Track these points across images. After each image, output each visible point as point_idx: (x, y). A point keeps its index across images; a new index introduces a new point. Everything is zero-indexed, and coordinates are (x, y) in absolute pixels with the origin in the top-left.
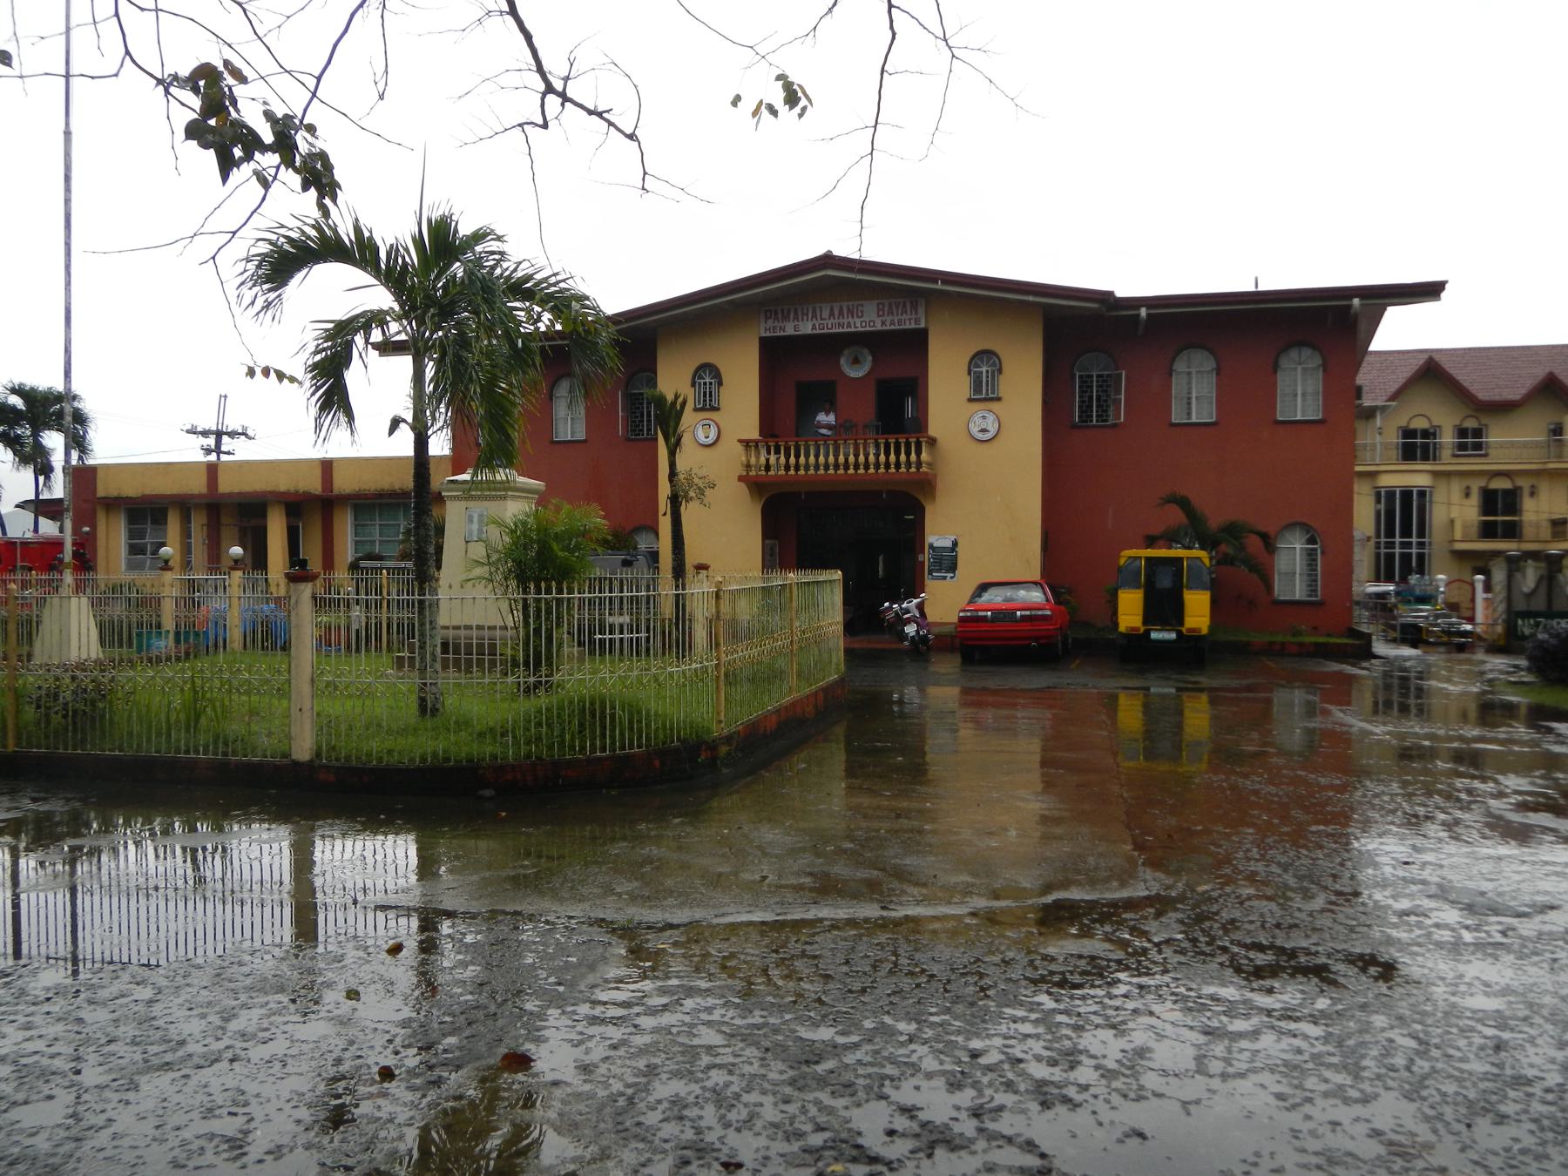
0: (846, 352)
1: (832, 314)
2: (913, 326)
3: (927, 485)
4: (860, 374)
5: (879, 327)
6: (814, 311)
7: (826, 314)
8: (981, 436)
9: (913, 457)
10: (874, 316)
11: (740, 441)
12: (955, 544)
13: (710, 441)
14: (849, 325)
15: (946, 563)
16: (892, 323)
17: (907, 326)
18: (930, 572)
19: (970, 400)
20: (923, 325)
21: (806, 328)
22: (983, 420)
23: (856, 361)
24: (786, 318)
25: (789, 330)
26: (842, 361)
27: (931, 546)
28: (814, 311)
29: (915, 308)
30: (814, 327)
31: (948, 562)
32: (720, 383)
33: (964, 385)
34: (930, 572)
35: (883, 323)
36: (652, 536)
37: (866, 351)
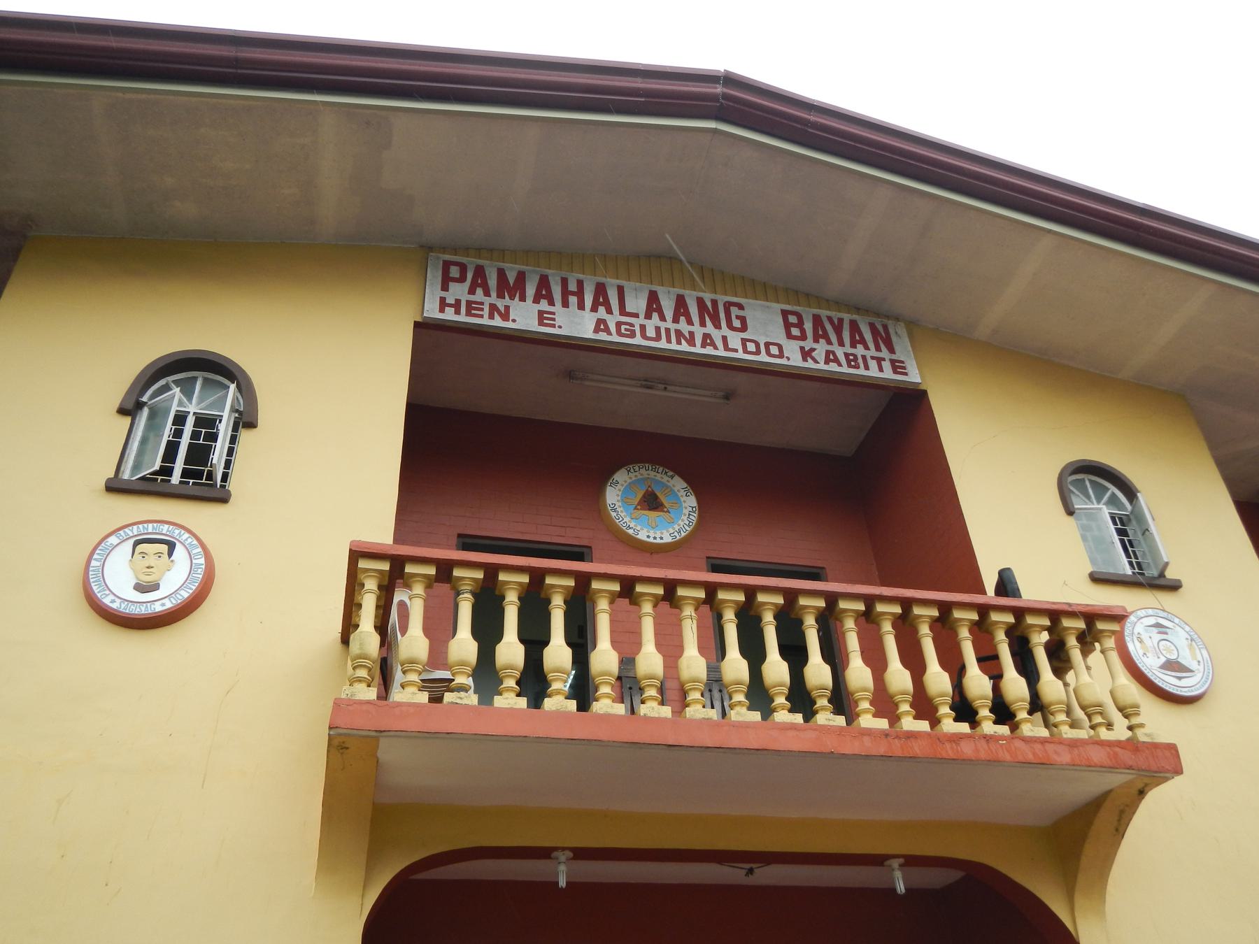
0: (621, 476)
1: (653, 304)
2: (888, 374)
5: (793, 357)
6: (601, 290)
7: (636, 303)
8: (1168, 681)
13: (159, 602)
16: (830, 357)
17: (874, 372)
20: (914, 376)
21: (577, 323)
23: (651, 502)
28: (601, 290)
30: (601, 325)
32: (246, 420)
35: (806, 354)
37: (678, 484)
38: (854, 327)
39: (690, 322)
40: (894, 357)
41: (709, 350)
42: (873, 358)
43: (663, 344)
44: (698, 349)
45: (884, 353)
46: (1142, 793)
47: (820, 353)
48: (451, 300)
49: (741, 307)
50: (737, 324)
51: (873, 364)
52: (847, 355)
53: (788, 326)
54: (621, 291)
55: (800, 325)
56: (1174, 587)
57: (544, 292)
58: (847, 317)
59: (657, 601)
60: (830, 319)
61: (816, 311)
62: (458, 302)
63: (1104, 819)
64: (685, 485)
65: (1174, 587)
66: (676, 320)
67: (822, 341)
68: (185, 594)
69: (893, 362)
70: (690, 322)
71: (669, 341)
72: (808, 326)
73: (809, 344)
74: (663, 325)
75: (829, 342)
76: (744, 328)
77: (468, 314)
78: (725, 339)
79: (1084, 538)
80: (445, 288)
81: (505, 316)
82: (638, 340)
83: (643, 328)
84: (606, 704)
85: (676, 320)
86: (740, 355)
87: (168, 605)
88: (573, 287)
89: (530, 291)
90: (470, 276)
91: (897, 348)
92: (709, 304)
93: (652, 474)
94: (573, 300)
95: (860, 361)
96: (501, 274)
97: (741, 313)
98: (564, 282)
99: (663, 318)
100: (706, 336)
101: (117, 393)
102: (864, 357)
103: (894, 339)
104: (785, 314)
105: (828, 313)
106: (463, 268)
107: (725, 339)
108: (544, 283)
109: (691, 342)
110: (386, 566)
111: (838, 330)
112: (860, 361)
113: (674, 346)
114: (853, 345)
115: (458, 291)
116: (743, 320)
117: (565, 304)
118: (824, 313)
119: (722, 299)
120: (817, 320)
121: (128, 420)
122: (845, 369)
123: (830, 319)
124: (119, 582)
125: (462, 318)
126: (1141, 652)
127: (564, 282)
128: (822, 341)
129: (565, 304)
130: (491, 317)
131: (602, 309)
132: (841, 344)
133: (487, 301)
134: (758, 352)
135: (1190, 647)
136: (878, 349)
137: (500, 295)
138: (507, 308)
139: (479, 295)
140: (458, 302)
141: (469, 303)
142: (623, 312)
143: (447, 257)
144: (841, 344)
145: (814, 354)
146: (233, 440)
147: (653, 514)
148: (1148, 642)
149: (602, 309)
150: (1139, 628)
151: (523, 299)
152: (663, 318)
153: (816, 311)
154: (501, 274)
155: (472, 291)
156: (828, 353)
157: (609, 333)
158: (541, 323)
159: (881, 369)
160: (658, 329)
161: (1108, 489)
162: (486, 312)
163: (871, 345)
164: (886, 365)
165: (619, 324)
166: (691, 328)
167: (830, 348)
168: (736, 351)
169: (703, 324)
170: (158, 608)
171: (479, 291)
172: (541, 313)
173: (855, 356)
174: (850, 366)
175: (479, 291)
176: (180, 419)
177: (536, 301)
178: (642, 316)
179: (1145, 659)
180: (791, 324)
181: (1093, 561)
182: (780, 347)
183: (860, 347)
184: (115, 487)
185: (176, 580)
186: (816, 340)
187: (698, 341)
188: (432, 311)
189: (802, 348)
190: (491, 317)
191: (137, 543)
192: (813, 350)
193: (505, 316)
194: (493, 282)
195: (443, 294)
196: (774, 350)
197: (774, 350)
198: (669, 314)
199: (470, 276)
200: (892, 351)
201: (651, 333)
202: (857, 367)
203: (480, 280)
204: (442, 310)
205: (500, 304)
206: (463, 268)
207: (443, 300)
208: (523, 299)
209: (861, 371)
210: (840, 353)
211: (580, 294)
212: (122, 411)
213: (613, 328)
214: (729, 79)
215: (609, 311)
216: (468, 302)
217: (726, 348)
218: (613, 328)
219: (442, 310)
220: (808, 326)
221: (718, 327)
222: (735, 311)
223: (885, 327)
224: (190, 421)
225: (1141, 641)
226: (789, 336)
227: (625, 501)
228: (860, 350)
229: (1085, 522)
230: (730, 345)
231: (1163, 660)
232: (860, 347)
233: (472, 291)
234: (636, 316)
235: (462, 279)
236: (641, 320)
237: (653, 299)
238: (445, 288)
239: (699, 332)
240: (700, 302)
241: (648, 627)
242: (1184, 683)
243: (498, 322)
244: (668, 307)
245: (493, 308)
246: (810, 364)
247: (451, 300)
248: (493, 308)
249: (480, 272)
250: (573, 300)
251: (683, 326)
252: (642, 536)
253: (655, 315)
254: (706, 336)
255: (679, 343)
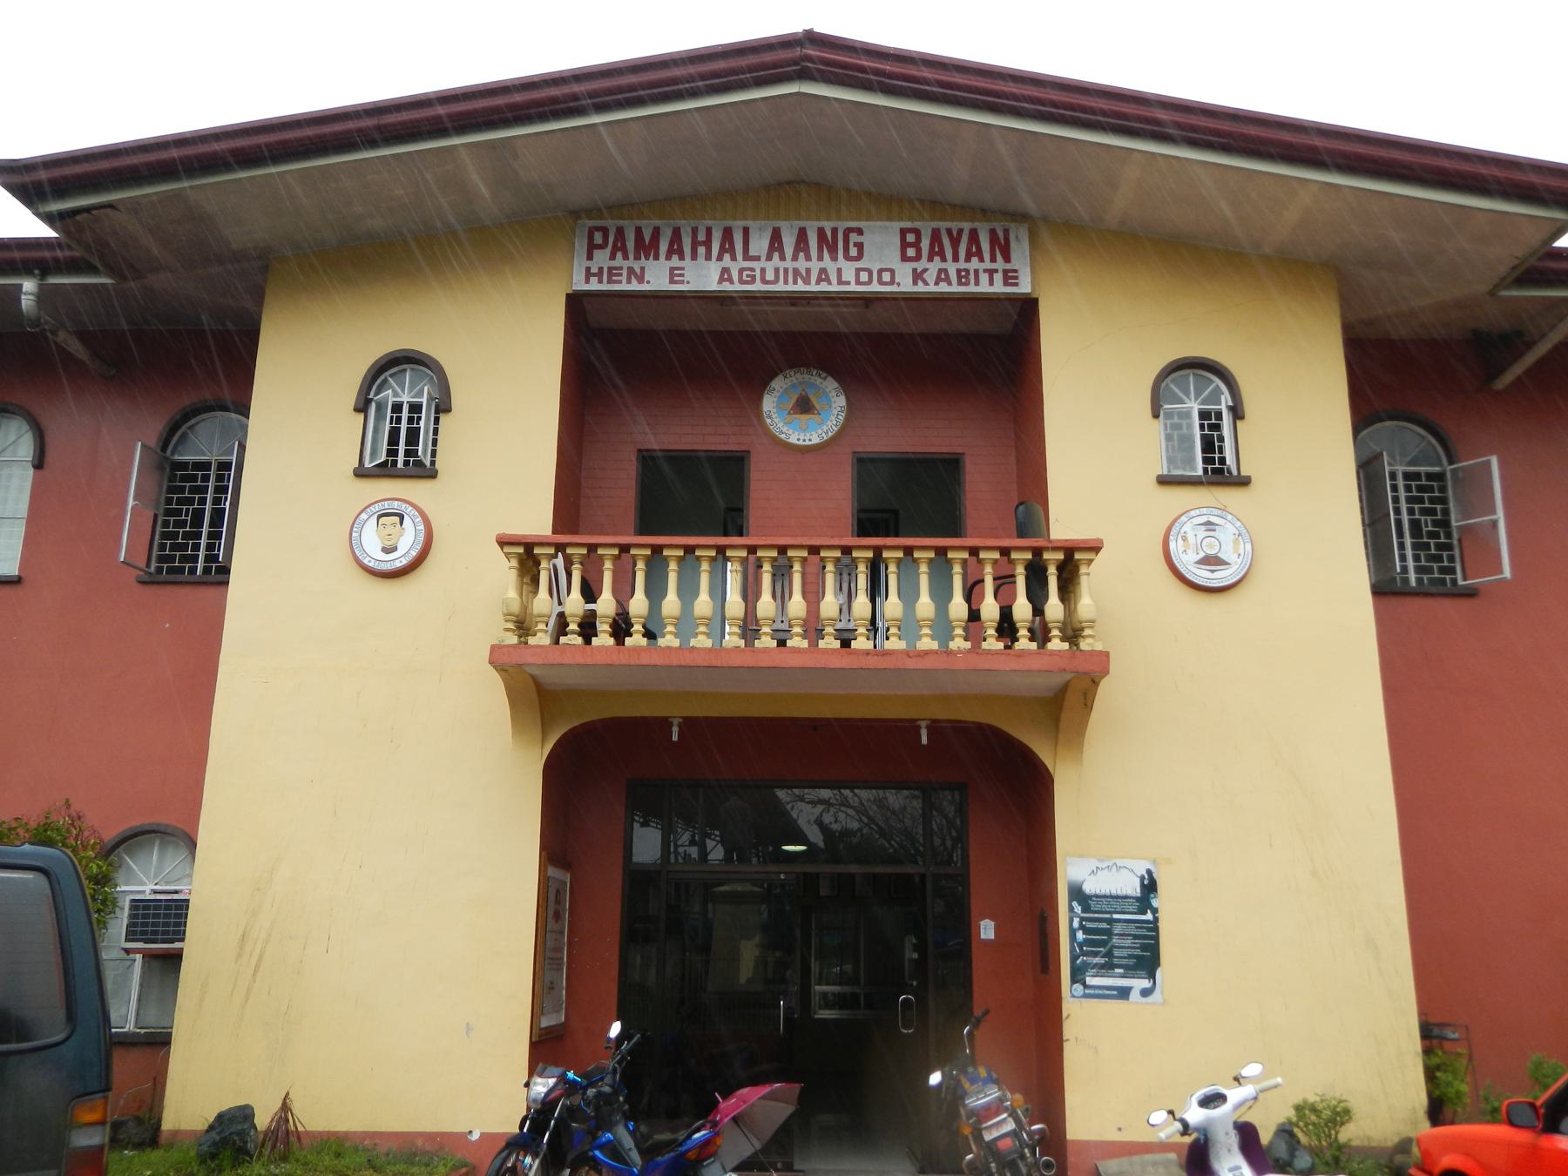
0: (778, 384)
2: (999, 287)
3: (1069, 698)
4: (814, 438)
6: (728, 234)
7: (759, 245)
8: (1202, 576)
9: (1054, 607)
10: (892, 259)
11: (503, 542)
12: (1150, 886)
13: (399, 560)
14: (823, 275)
15: (1124, 946)
16: (942, 276)
17: (984, 287)
18: (1077, 975)
19: (1163, 481)
20: (1025, 287)
21: (704, 276)
22: (1209, 528)
23: (804, 406)
24: (646, 248)
25: (657, 277)
26: (769, 403)
27: (1077, 893)
28: (728, 234)
29: (1003, 248)
30: (725, 275)
31: (1132, 943)
33: (1148, 446)
34: (1077, 975)
35: (918, 276)
36: (183, 853)
37: (831, 385)
38: (974, 236)
39: (808, 258)
40: (1008, 267)
41: (824, 287)
42: (985, 271)
43: (780, 287)
44: (813, 288)
45: (1000, 264)
46: (1095, 683)
47: (931, 276)
48: (594, 270)
49: (860, 232)
50: (853, 252)
51: (984, 278)
52: (959, 271)
53: (904, 245)
54: (746, 231)
55: (917, 245)
56: (1244, 482)
57: (675, 249)
58: (967, 226)
59: (712, 560)
60: (949, 231)
61: (935, 224)
62: (601, 269)
63: (1072, 699)
64: (836, 385)
65: (1244, 482)
66: (795, 258)
67: (937, 259)
68: (414, 553)
69: (1005, 272)
70: (808, 258)
71: (786, 282)
72: (925, 244)
73: (919, 266)
74: (782, 265)
75: (944, 259)
76: (860, 257)
77: (610, 281)
78: (839, 271)
79: (1169, 438)
80: (590, 257)
81: (641, 279)
82: (758, 286)
83: (763, 271)
84: (668, 640)
85: (795, 258)
86: (853, 288)
87: (404, 562)
88: (701, 237)
89: (663, 247)
90: (611, 239)
91: (1013, 256)
92: (829, 234)
93: (807, 377)
94: (702, 250)
95: (972, 277)
96: (639, 231)
97: (859, 239)
98: (695, 231)
99: (783, 258)
100: (823, 271)
101: (351, 397)
102: (976, 272)
103: (1013, 245)
104: (903, 232)
105: (948, 224)
106: (605, 231)
107: (839, 271)
108: (676, 236)
109: (807, 281)
110: (521, 550)
111: (955, 243)
112: (972, 277)
113: (791, 287)
114: (968, 260)
115: (602, 258)
116: (860, 246)
117: (694, 257)
118: (943, 225)
119: (843, 225)
120: (936, 237)
121: (362, 416)
122: (955, 288)
123: (949, 231)
124: (371, 544)
125: (605, 287)
126: (1181, 549)
127: (695, 231)
128: (937, 259)
129: (694, 257)
130: (629, 281)
131: (727, 257)
132: (956, 259)
133: (626, 264)
134: (870, 282)
135: (1236, 542)
136: (993, 260)
137: (637, 258)
138: (643, 269)
139: (619, 261)
140: (601, 269)
141: (610, 269)
142: (747, 257)
143: (592, 223)
144: (956, 259)
145: (925, 276)
146: (437, 420)
147: (804, 418)
148: (1191, 539)
149: (727, 257)
150: (1187, 528)
151: (657, 257)
152: (783, 258)
153: (935, 224)
154: (639, 231)
155: (613, 257)
156: (940, 271)
157: (732, 282)
158: (672, 281)
159: (991, 283)
160: (777, 270)
161: (1212, 382)
162: (624, 278)
163: (987, 256)
164: (998, 277)
165: (741, 271)
166: (808, 264)
167: (943, 266)
168: (848, 283)
169: (820, 258)
170: (398, 564)
171: (619, 255)
172: (672, 269)
173: (967, 271)
174: (960, 283)
175: (619, 255)
176: (397, 408)
177: (668, 258)
178: (763, 258)
179: (1183, 557)
180: (908, 245)
181: (1170, 461)
182: (892, 272)
183: (975, 260)
184: (361, 473)
185: (408, 542)
186: (930, 259)
187: (814, 279)
188: (582, 286)
189: (915, 270)
190: (629, 281)
191: (379, 517)
192: (925, 270)
193: (641, 279)
194: (631, 244)
195: (589, 264)
196: (886, 277)
197: (886, 277)
198: (789, 251)
199: (611, 239)
200: (1007, 259)
201: (770, 276)
202: (967, 284)
203: (620, 247)
204: (587, 281)
205: (637, 267)
206: (605, 231)
207: (588, 269)
208: (657, 257)
209: (972, 288)
210: (952, 269)
211: (708, 244)
212: (357, 410)
213: (735, 277)
214: (812, 38)
215: (734, 258)
216: (610, 269)
217: (840, 282)
218: (735, 277)
219: (587, 281)
220: (925, 244)
221: (834, 258)
222: (854, 238)
223: (1006, 232)
224: (405, 408)
225: (1185, 539)
226: (904, 258)
227: (779, 408)
228: (975, 263)
229: (1176, 420)
230: (844, 276)
231: (1202, 555)
232: (975, 260)
233: (613, 257)
234: (758, 258)
235: (602, 247)
236: (763, 263)
237: (776, 237)
238: (590, 257)
239: (815, 266)
240: (821, 232)
241: (704, 580)
242: (1217, 575)
243: (635, 286)
244: (789, 242)
245: (631, 271)
246: (921, 288)
247: (594, 270)
248: (631, 271)
249: (620, 232)
250: (702, 250)
251: (802, 264)
252: (793, 440)
253: (776, 256)
254: (823, 271)
255: (795, 282)
